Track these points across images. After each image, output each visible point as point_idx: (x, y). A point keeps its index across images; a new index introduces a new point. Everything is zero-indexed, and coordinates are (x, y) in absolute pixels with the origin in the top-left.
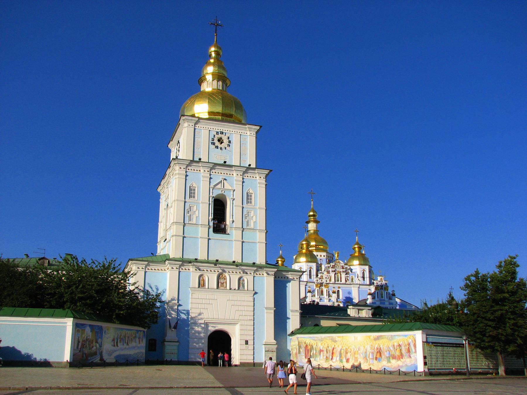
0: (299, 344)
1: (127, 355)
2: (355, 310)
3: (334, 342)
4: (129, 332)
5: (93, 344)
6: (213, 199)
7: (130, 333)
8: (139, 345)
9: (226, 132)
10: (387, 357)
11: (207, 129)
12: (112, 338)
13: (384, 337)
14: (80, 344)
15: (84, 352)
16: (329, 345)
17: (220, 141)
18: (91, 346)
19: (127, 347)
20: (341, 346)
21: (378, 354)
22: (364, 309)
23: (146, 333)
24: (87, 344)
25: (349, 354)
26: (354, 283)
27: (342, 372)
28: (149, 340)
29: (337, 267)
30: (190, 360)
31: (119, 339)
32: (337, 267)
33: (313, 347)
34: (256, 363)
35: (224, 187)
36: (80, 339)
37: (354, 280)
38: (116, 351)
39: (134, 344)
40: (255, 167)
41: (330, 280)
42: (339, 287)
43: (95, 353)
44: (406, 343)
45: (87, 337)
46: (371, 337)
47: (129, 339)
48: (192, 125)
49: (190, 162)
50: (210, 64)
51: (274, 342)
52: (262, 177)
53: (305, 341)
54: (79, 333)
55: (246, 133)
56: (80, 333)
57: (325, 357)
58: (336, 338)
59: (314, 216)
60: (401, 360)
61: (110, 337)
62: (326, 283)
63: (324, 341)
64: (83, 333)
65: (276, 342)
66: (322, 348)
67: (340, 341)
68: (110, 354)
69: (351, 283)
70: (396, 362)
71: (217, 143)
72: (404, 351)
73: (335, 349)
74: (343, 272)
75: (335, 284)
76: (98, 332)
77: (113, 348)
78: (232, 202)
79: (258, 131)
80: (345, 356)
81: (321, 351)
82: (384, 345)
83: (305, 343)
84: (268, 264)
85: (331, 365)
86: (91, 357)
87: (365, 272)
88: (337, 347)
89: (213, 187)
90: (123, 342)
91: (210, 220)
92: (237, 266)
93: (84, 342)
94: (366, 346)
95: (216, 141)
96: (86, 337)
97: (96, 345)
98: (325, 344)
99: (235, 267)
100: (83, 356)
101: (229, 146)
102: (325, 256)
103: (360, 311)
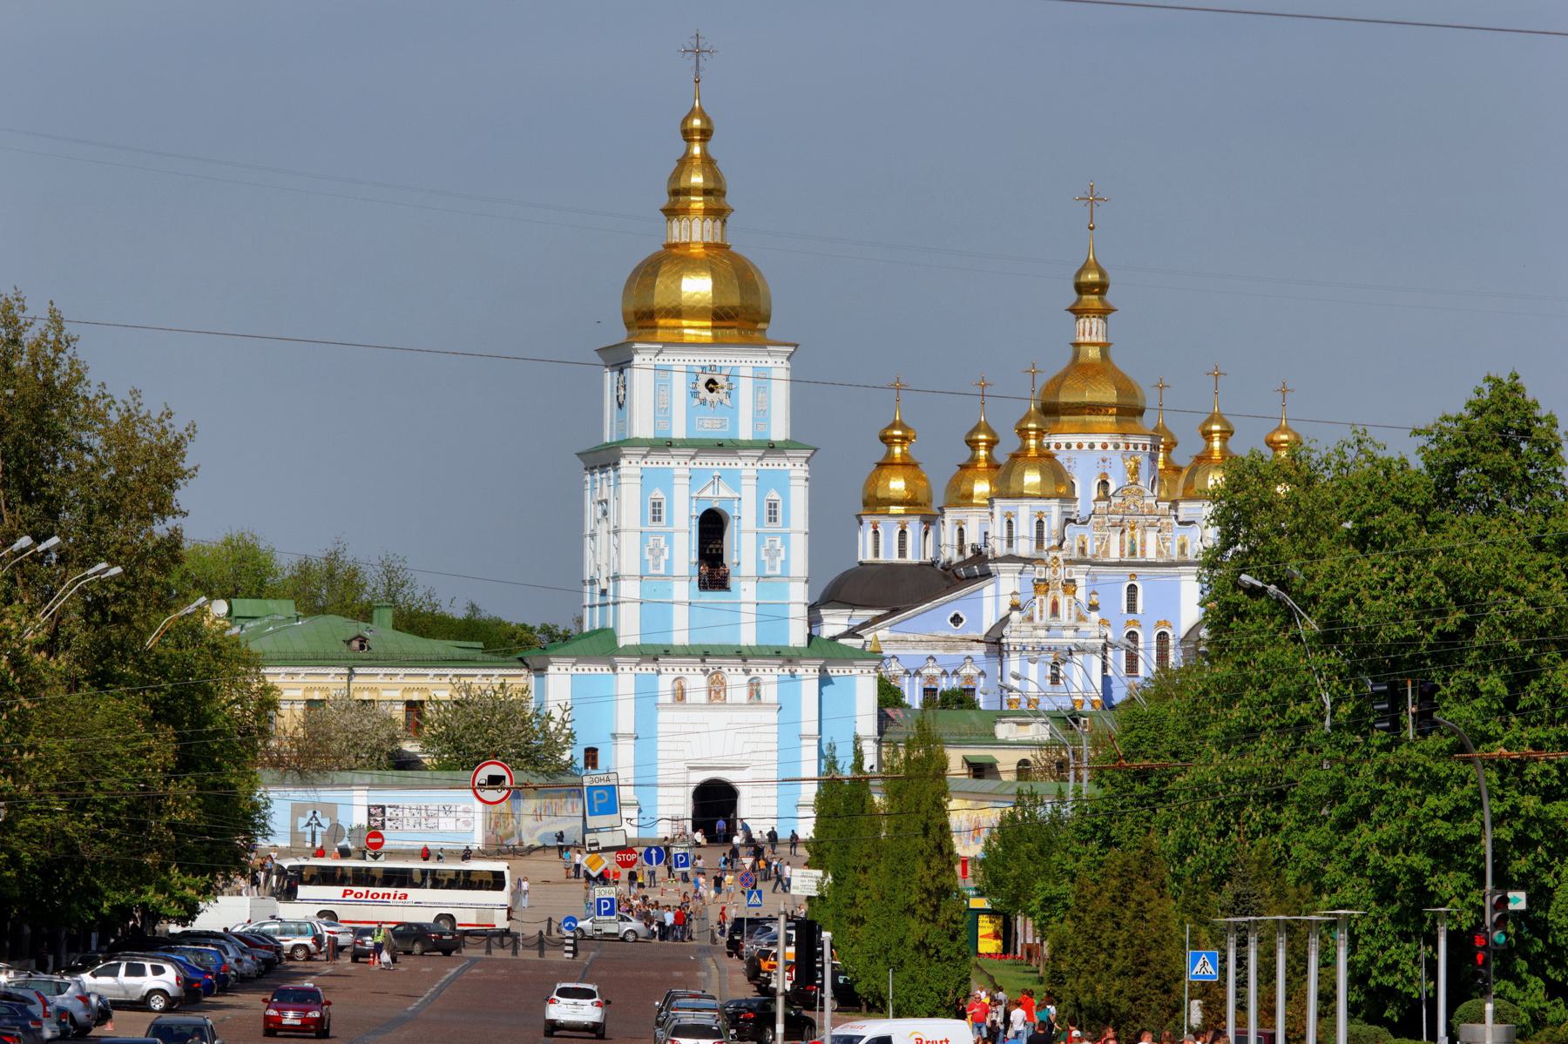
9: (722, 364)
17: (711, 385)
37: (1188, 551)
41: (1106, 553)
42: (1133, 576)
43: (512, 834)
52: (798, 465)
62: (1067, 581)
68: (531, 834)
69: (1176, 557)
71: (704, 393)
74: (1152, 525)
75: (1119, 564)
79: (792, 354)
92: (745, 660)
102: (1122, 445)
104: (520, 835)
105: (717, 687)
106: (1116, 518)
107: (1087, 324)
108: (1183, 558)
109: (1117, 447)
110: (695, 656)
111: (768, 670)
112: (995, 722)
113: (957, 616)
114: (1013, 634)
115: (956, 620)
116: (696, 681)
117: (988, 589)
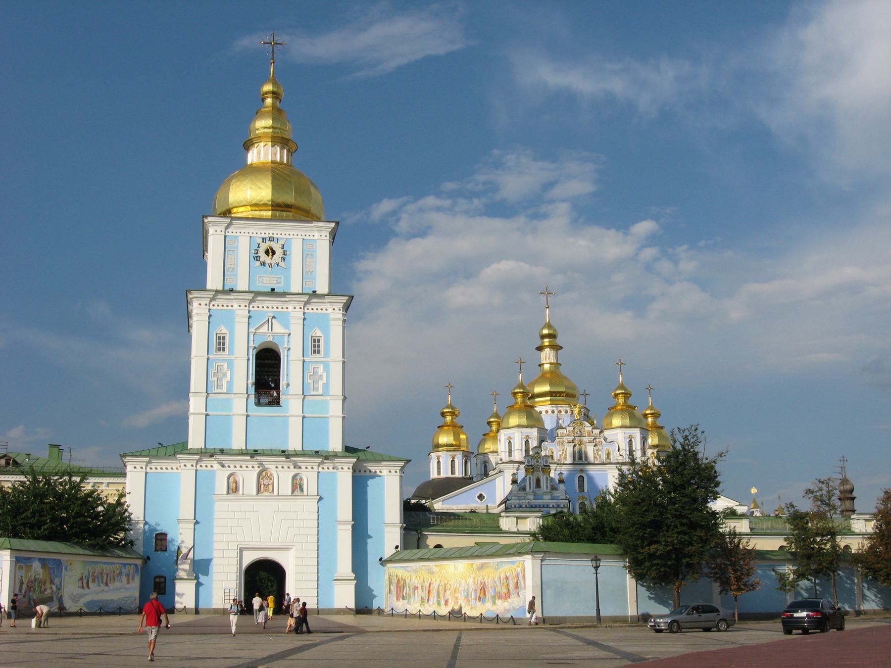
0: (389, 578)
1: (107, 601)
2: (510, 518)
3: (431, 573)
4: (109, 566)
6: (255, 351)
7: (109, 568)
9: (279, 236)
10: (492, 596)
11: (247, 234)
12: (78, 576)
13: (489, 565)
14: (24, 587)
16: (425, 580)
17: (270, 252)
19: (106, 588)
20: (438, 580)
21: (483, 590)
22: (528, 517)
23: (139, 567)
24: (36, 587)
25: (448, 592)
26: (612, 461)
27: (390, 618)
28: (155, 578)
29: (578, 433)
30: (214, 606)
31: (92, 577)
32: (578, 433)
33: (406, 582)
34: (321, 609)
35: (272, 330)
37: (611, 457)
38: (85, 595)
39: (117, 584)
40: (326, 291)
41: (565, 458)
44: (514, 574)
45: (35, 576)
46: (474, 565)
47: (109, 578)
48: (222, 231)
49: (215, 294)
50: (263, 115)
51: (353, 576)
52: (337, 309)
53: (397, 574)
54: (22, 571)
55: (313, 236)
56: (24, 571)
57: (421, 597)
58: (434, 567)
59: (550, 336)
60: (508, 600)
62: (545, 466)
63: (418, 574)
65: (354, 575)
66: (417, 584)
67: (438, 572)
68: (75, 599)
70: (503, 603)
71: (263, 257)
72: (512, 587)
73: (432, 585)
74: (590, 442)
76: (54, 568)
77: (81, 591)
78: (286, 354)
80: (444, 595)
81: (416, 588)
82: (489, 578)
83: (397, 576)
84: (349, 450)
85: (420, 611)
87: (632, 439)
88: (434, 581)
89: (254, 331)
90: (99, 582)
91: (250, 385)
92: (288, 457)
94: (468, 580)
95: (262, 254)
96: (33, 576)
98: (420, 576)
99: (285, 459)
100: (30, 603)
101: (284, 260)
103: (519, 520)
104: (60, 600)
105: (266, 482)
106: (571, 438)
107: (548, 352)
108: (608, 461)
109: (566, 412)
110: (246, 454)
111: (309, 467)
112: (501, 516)
113: (481, 495)
114: (513, 498)
115: (481, 497)
116: (248, 476)
117: (499, 481)
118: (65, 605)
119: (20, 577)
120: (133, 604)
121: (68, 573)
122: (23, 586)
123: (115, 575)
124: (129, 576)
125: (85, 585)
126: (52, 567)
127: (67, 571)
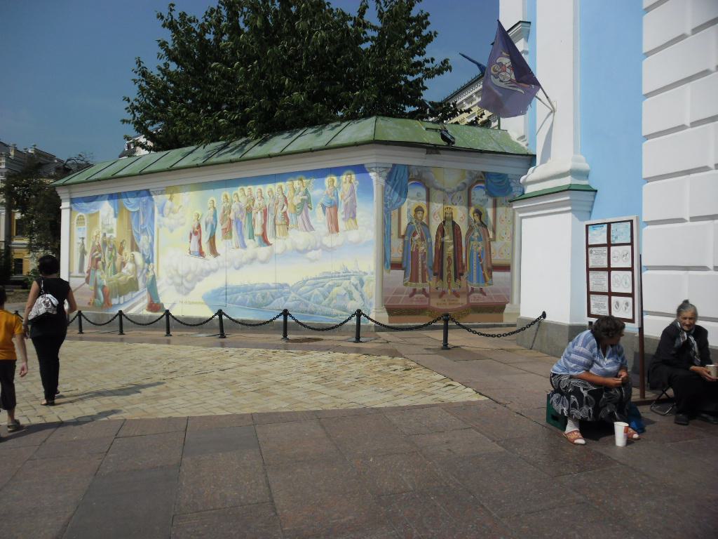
1: (268, 287)
4: (270, 186)
5: (124, 256)
7: (271, 191)
8: (329, 241)
12: (190, 225)
14: (87, 259)
15: (98, 283)
18: (118, 263)
19: (263, 251)
24: (107, 260)
36: (85, 243)
38: (208, 273)
39: (298, 237)
45: (105, 235)
56: (85, 227)
61: (183, 225)
64: (93, 225)
68: (184, 284)
76: (138, 212)
86: (120, 296)
90: (241, 235)
93: (97, 252)
96: (101, 235)
97: (134, 257)
100: (96, 296)
104: (152, 287)
118: (161, 301)
119: (80, 241)
120: (352, 299)
121: (166, 220)
122: (85, 257)
123: (289, 210)
124: (335, 206)
125: (206, 248)
126: (133, 210)
127: (163, 216)
